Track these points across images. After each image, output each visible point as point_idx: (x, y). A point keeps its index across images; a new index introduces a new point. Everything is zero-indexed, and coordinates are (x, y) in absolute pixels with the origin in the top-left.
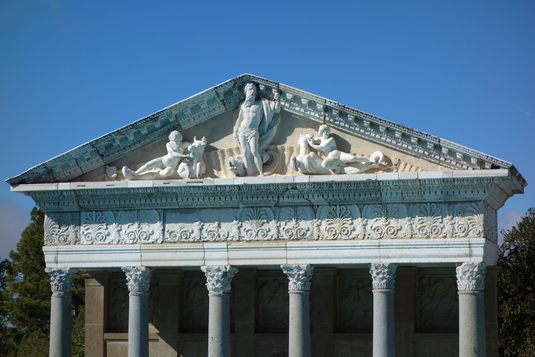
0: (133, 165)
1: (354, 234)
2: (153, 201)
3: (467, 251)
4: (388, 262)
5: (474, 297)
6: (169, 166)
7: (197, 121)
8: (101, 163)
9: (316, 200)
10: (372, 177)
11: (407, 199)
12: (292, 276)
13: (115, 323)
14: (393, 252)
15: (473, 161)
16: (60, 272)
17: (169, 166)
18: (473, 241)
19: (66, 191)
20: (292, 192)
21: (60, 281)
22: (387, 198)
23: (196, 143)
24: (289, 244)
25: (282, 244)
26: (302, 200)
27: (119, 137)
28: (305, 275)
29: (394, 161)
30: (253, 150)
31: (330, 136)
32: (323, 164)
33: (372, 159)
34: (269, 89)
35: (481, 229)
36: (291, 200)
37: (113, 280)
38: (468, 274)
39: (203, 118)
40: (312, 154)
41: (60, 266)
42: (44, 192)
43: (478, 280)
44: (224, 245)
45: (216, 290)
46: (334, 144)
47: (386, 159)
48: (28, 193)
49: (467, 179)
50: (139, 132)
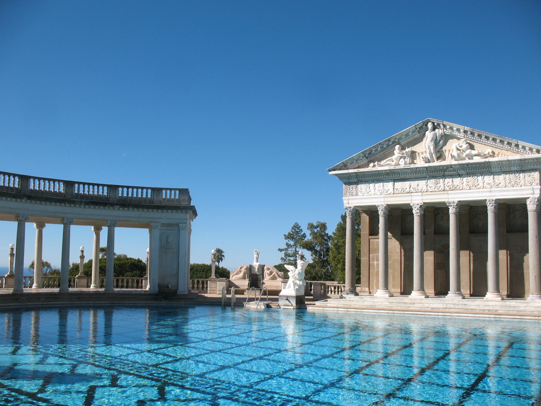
0: (380, 160)
1: (479, 187)
3: (532, 192)
4: (495, 198)
5: (536, 212)
6: (396, 160)
7: (408, 140)
8: (366, 161)
9: (461, 172)
10: (487, 160)
12: (450, 206)
13: (374, 232)
14: (497, 194)
15: (534, 150)
16: (350, 208)
17: (396, 160)
18: (534, 187)
19: (352, 173)
20: (450, 169)
21: (350, 211)
22: (493, 170)
23: (407, 150)
24: (449, 192)
25: (446, 192)
26: (455, 173)
27: (374, 149)
28: (457, 205)
29: (496, 153)
30: (432, 151)
31: (467, 143)
32: (464, 156)
33: (486, 153)
34: (439, 125)
35: (538, 182)
36: (450, 173)
37: (372, 212)
38: (533, 202)
39: (410, 139)
40: (459, 152)
41: (350, 205)
42: (343, 174)
43: (537, 205)
44: (420, 194)
45: (417, 213)
46: (469, 147)
47: (493, 153)
48: (336, 175)
49: (531, 159)
50: (382, 147)
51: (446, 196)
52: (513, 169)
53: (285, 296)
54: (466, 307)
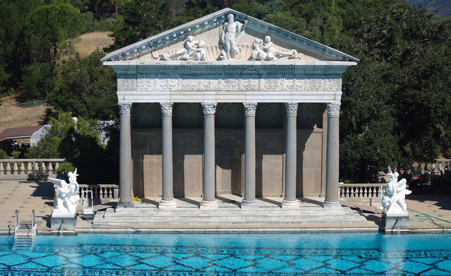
2: (178, 70)
11: (306, 72)
14: (298, 97)
18: (337, 93)
24: (247, 93)
36: (249, 72)
44: (214, 93)
51: (244, 97)
52: (316, 72)
53: (60, 218)
54: (268, 219)
